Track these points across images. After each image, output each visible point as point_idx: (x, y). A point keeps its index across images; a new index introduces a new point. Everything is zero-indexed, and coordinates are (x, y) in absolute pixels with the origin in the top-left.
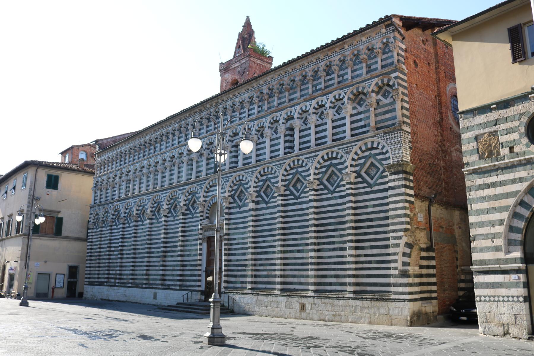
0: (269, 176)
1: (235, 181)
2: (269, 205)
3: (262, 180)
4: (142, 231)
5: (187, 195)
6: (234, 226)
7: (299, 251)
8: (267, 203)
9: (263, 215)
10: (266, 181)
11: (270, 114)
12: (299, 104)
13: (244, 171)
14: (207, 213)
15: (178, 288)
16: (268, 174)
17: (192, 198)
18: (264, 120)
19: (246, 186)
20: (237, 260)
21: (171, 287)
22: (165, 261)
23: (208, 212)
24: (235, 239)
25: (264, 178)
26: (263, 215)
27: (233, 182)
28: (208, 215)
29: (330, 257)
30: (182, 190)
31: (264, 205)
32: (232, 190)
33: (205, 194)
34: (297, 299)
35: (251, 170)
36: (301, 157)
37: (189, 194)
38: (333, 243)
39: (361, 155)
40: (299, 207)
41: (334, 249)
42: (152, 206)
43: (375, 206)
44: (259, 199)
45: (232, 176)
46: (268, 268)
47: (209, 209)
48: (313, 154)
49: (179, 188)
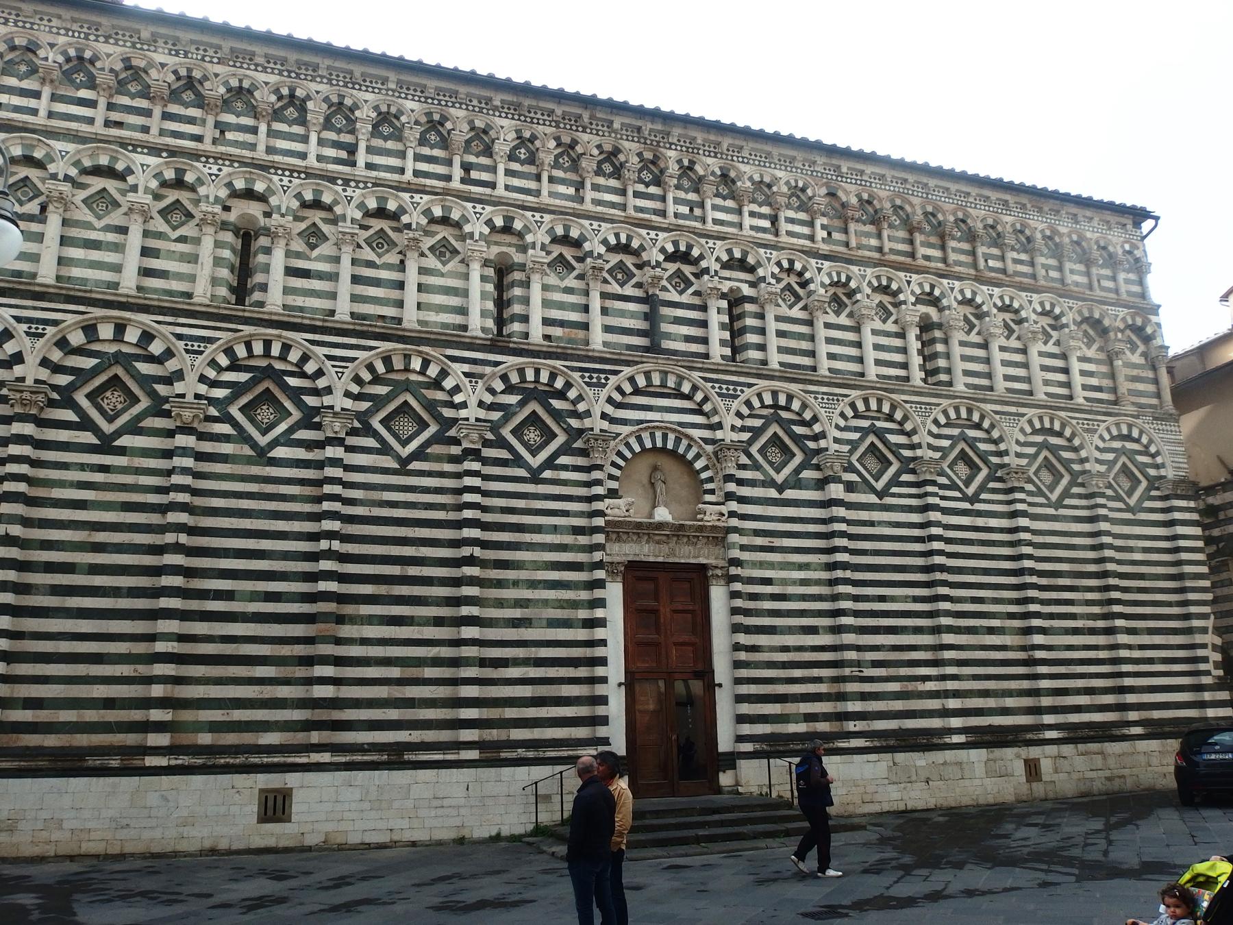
0: (879, 424)
1: (756, 404)
2: (888, 500)
3: (856, 429)
4: (99, 477)
5: (499, 386)
6: (759, 541)
7: (991, 631)
8: (880, 495)
9: (872, 524)
10: (865, 432)
11: (876, 265)
12: (960, 279)
13: (801, 386)
14: (611, 477)
15: (473, 754)
16: (878, 419)
17: (522, 404)
18: (855, 269)
19: (799, 430)
20: (785, 649)
21: (408, 757)
22: (339, 641)
23: (617, 473)
24: (768, 581)
25: (865, 424)
26: (872, 524)
27: (748, 403)
28: (614, 485)
29: (1070, 648)
30: (474, 362)
31: (873, 499)
32: (743, 429)
33: (609, 410)
34: (1016, 750)
35: (825, 389)
36: (982, 405)
37: (510, 389)
38: (1073, 616)
39: (1107, 445)
40: (980, 522)
41: (1076, 631)
42: (211, 374)
43: (1146, 550)
44: (853, 477)
45: (750, 385)
46: (904, 671)
47: (622, 463)
48: (1013, 409)
49: (450, 352)
